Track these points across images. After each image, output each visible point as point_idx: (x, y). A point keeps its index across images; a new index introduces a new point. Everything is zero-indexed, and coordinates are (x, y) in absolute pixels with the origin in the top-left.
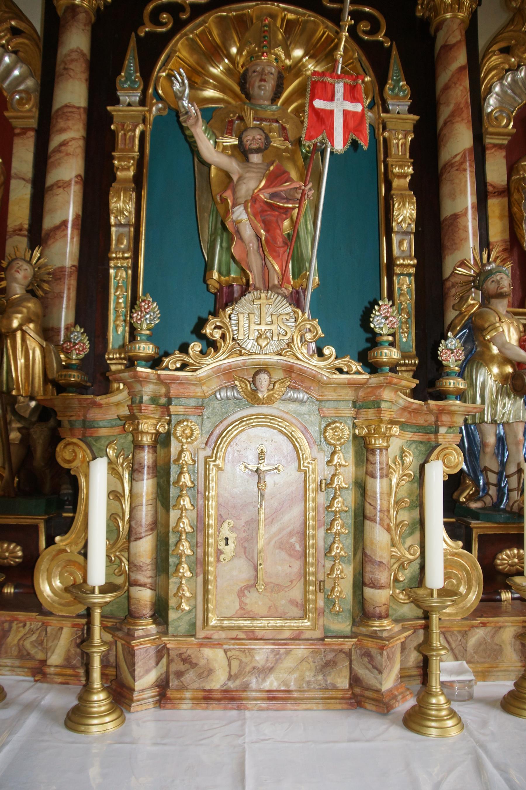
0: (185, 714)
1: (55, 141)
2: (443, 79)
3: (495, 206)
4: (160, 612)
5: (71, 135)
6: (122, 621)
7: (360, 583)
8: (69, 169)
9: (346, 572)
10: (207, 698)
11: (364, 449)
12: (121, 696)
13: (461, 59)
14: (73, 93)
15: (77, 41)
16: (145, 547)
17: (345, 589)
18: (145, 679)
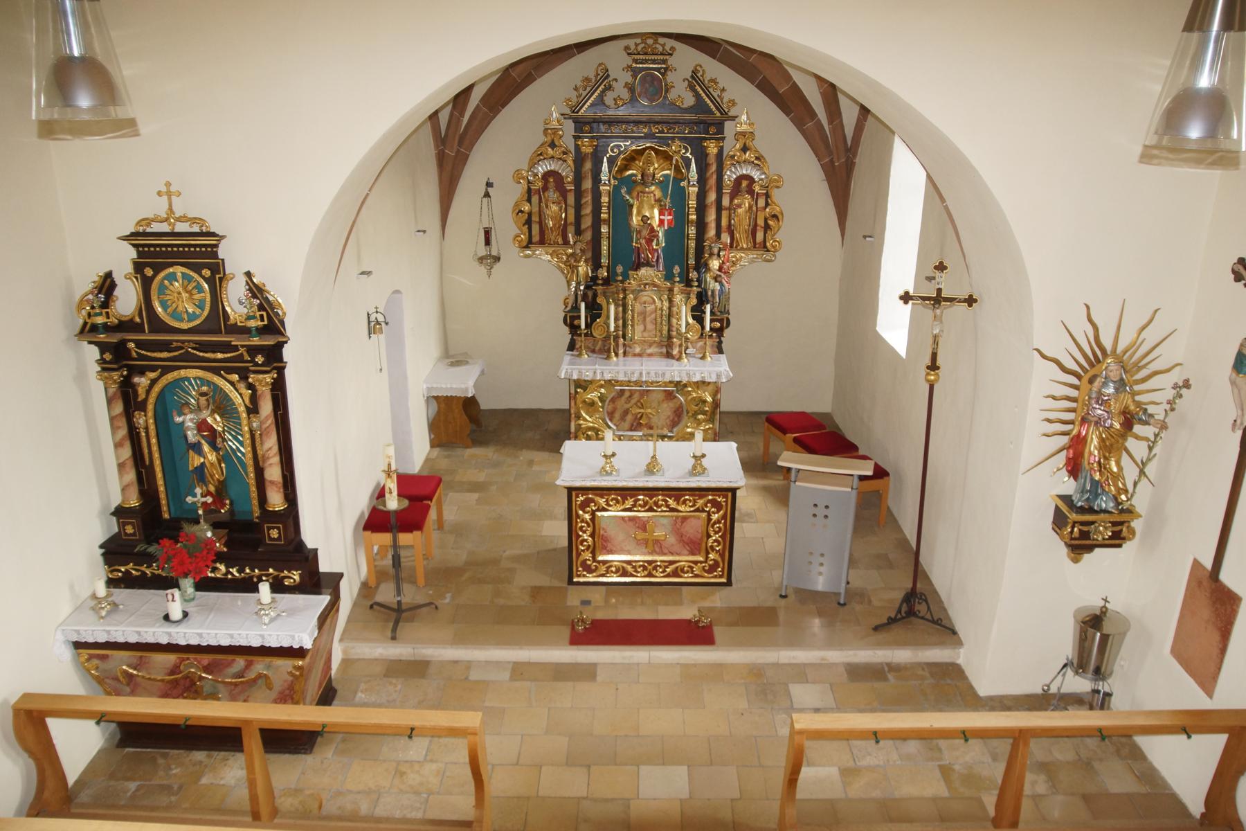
0: (630, 359)
1: (583, 201)
2: (708, 174)
3: (725, 214)
4: (624, 337)
5: (588, 198)
6: (616, 338)
7: (669, 330)
8: (587, 210)
9: (666, 328)
10: (635, 355)
11: (670, 301)
12: (617, 355)
13: (714, 168)
14: (587, 184)
15: (588, 165)
16: (621, 322)
17: (665, 332)
18: (621, 351)
